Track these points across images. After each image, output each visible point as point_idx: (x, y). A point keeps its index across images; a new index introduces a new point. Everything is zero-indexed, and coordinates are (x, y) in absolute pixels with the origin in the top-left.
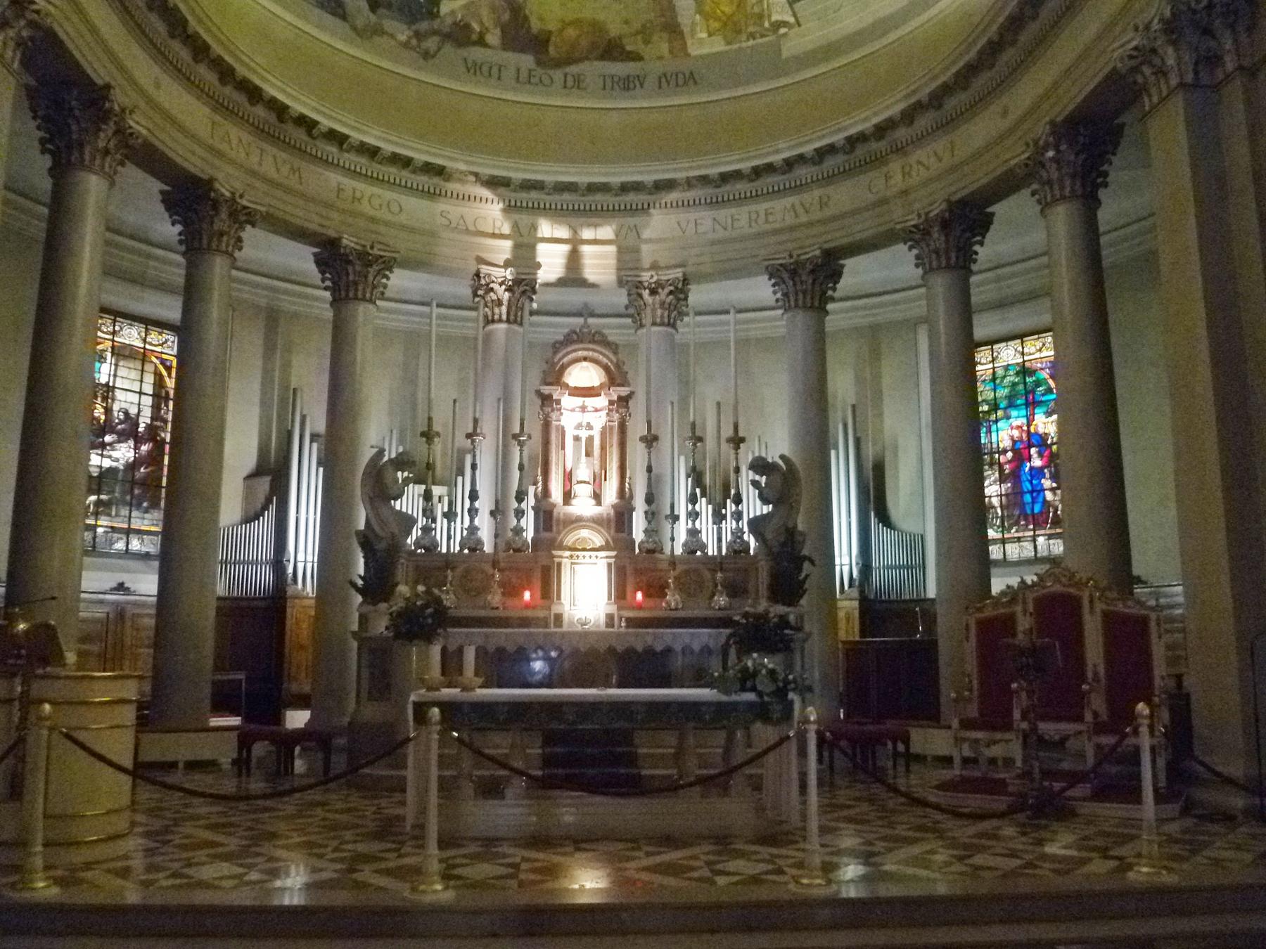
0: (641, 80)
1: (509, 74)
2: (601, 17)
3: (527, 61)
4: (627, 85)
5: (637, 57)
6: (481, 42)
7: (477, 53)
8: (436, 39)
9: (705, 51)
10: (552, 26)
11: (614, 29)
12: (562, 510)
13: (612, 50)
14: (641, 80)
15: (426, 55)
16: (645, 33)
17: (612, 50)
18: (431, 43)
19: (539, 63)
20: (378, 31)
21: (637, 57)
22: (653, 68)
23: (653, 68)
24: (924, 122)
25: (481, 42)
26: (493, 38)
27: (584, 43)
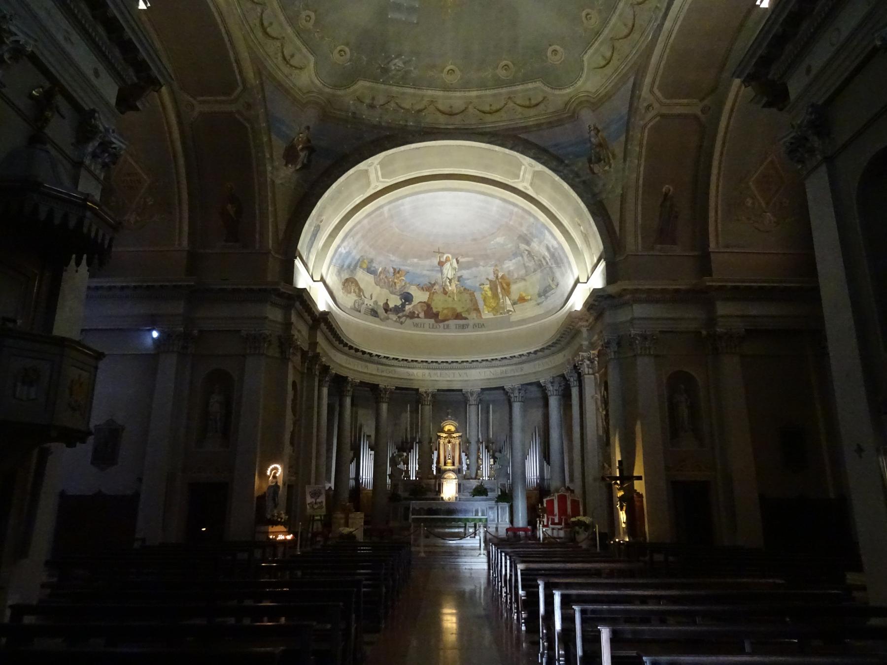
0: (468, 325)
1: (427, 326)
2: (455, 306)
3: (432, 321)
4: (463, 327)
5: (466, 319)
6: (418, 317)
7: (416, 320)
10: (440, 310)
11: (459, 310)
12: (444, 467)
13: (458, 316)
14: (468, 325)
15: (402, 323)
17: (458, 316)
18: (403, 319)
19: (436, 322)
20: (388, 318)
21: (466, 319)
22: (471, 322)
24: (547, 352)
26: (422, 315)
27: (450, 314)
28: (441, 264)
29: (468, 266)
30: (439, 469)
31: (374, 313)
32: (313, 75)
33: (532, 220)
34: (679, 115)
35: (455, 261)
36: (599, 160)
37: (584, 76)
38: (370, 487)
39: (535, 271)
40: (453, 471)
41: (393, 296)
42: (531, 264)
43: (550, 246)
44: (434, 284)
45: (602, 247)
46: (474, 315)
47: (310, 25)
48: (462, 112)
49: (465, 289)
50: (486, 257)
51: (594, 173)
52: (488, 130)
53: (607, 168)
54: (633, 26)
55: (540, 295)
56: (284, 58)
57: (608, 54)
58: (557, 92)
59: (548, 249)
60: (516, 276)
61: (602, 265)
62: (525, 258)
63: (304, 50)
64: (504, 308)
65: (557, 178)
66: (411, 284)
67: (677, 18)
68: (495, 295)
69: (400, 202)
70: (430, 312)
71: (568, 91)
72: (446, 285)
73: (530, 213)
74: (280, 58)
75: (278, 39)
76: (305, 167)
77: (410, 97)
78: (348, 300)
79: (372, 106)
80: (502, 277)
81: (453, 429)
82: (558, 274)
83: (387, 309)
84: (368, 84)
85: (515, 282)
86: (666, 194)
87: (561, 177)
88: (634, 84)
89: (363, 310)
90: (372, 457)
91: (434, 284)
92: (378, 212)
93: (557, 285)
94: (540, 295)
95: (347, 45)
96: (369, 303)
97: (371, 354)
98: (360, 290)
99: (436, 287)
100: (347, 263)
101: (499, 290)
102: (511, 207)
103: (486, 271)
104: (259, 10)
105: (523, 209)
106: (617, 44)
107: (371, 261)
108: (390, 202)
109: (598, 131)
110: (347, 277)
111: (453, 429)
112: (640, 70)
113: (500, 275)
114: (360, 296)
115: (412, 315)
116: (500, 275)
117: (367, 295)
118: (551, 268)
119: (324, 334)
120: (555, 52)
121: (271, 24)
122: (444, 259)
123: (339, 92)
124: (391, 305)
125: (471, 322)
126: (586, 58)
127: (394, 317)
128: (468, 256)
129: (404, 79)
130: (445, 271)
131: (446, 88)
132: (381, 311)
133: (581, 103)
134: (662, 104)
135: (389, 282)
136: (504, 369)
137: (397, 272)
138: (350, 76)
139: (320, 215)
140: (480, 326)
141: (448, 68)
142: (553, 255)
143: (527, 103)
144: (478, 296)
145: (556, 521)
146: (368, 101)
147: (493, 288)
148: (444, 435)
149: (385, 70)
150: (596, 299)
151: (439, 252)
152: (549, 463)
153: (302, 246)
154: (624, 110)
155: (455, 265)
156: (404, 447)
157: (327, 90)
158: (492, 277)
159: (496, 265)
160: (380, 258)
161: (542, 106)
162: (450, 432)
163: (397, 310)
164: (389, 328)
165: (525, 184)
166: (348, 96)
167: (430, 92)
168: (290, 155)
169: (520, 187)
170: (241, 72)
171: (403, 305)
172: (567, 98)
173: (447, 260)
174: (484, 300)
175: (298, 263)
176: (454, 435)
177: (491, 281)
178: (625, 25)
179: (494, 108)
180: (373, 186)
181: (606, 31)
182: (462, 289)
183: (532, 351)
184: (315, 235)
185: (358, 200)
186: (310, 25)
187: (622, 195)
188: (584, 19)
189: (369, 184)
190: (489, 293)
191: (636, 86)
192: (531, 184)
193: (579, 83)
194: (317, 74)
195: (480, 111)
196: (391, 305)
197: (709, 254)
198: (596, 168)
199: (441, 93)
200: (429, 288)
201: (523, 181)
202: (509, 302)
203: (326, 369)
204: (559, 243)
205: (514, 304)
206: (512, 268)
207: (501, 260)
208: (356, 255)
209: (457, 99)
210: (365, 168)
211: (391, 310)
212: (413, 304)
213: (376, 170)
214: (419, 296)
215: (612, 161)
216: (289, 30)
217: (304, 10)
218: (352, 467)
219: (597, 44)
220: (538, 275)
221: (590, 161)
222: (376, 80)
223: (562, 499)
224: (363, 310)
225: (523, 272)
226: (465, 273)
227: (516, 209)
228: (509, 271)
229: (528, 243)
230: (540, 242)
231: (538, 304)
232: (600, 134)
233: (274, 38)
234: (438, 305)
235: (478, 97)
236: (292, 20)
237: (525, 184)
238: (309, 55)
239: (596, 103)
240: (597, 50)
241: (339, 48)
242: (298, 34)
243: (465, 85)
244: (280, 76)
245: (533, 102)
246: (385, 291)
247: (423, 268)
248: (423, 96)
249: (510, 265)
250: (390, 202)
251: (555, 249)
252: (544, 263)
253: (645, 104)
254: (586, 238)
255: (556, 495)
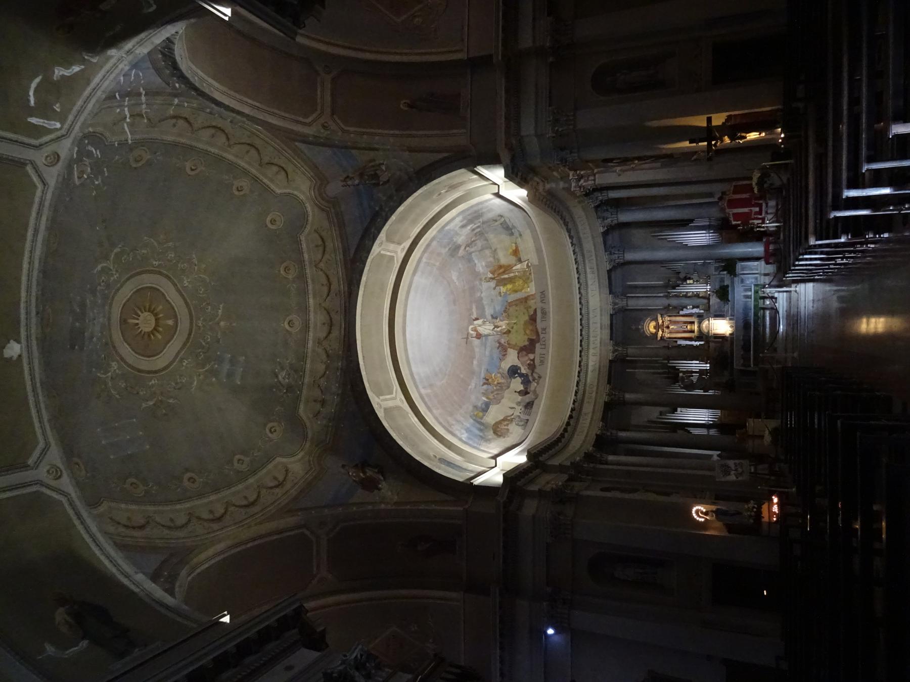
1: (544, 352)
2: (522, 322)
3: (538, 345)
4: (544, 313)
5: (535, 310)
6: (533, 360)
7: (537, 362)
8: (535, 375)
9: (534, 289)
10: (526, 337)
11: (527, 318)
12: (696, 333)
13: (533, 319)
15: (540, 377)
16: (527, 308)
17: (533, 319)
18: (535, 375)
20: (535, 391)
21: (535, 310)
22: (540, 305)
23: (539, 305)
24: (570, 226)
25: (533, 360)
26: (531, 356)
27: (531, 328)
28: (479, 336)
29: (481, 308)
30: (698, 338)
31: (529, 406)
32: (292, 459)
33: (434, 243)
34: (332, 95)
35: (476, 322)
36: (375, 176)
37: (295, 193)
38: (718, 412)
39: (486, 240)
40: (700, 323)
41: (512, 385)
42: (480, 244)
43: (461, 224)
44: (500, 343)
45: (463, 170)
46: (531, 303)
47: (247, 460)
48: (328, 313)
49: (505, 311)
50: (473, 289)
51: (388, 181)
52: (346, 289)
53: (384, 168)
54: (249, 144)
55: (512, 234)
56: (277, 487)
57: (275, 169)
58: (310, 218)
59: (463, 226)
60: (491, 259)
61: (482, 170)
62: (472, 250)
63: (270, 466)
64: (525, 272)
65: (393, 217)
66: (500, 367)
67: (241, 101)
68: (511, 280)
69: (416, 377)
70: (528, 348)
71: (309, 209)
72: (500, 331)
73: (428, 245)
74: (277, 490)
75: (259, 492)
76: (381, 472)
77: (315, 366)
78: (516, 432)
79: (323, 403)
80: (493, 273)
81: (653, 324)
82: (490, 215)
83: (525, 393)
84: (302, 407)
85: (498, 260)
86: (411, 106)
87: (391, 215)
88: (304, 142)
89: (527, 417)
90: (684, 410)
91: (500, 343)
92: (427, 400)
93: (501, 216)
94: (512, 234)
95: (265, 425)
96: (518, 410)
97: (573, 410)
98: (503, 420)
99: (503, 341)
100: (477, 432)
101: (506, 276)
102: (422, 265)
103: (486, 289)
104: (232, 509)
105: (424, 251)
106: (266, 159)
107: (475, 407)
108: (417, 387)
109: (348, 177)
110: (492, 432)
111: (653, 324)
112: (289, 138)
113: (490, 275)
114: (511, 420)
115: (532, 366)
116: (490, 275)
117: (510, 412)
118: (483, 223)
119: (553, 456)
120: (273, 222)
121: (245, 498)
122: (474, 333)
123: (310, 435)
124: (521, 388)
125: (540, 305)
126: (278, 191)
127: (534, 384)
128: (471, 309)
129: (297, 370)
130: (486, 332)
131: (306, 327)
132: (527, 398)
133: (320, 194)
134: (322, 112)
135: (497, 390)
136: (588, 270)
137: (487, 382)
138: (294, 423)
139: (428, 458)
140: (543, 295)
141: (287, 326)
142: (470, 221)
143: (321, 249)
144: (512, 297)
145: (757, 209)
146: (318, 406)
147: (502, 282)
148: (660, 332)
149: (290, 388)
150: (515, 175)
151: (467, 338)
152: (692, 221)
153: (460, 477)
154: (328, 152)
155: (480, 322)
156: (674, 376)
157: (308, 445)
158: (492, 284)
159: (481, 280)
160: (473, 397)
161: (324, 234)
162: (657, 327)
163: (526, 381)
164: (544, 391)
165: (399, 251)
166: (314, 427)
167: (310, 344)
168: (370, 485)
169: (401, 255)
170: (291, 529)
171: (521, 375)
172: (316, 210)
173: (475, 330)
174: (516, 291)
175: (478, 481)
176: (660, 322)
177: (497, 285)
178: (248, 152)
179: (325, 281)
180: (400, 404)
181: (254, 171)
182: (504, 315)
183: (569, 241)
184: (449, 464)
185: (415, 420)
186: (247, 460)
187: (410, 151)
188: (242, 193)
189: (398, 408)
190: (509, 286)
191: (305, 140)
192: (399, 244)
193: (302, 197)
194: (292, 455)
195: (328, 295)
196: (521, 388)
197: (469, 59)
198: (384, 178)
199: (311, 334)
200: (503, 349)
201: (396, 252)
202: (519, 266)
203: (588, 456)
204: (458, 215)
205: (520, 261)
206: (484, 264)
207: (475, 274)
208: (469, 423)
209: (316, 318)
210: (382, 410)
211: (526, 388)
212: (520, 365)
213: (383, 400)
214: (512, 359)
215: (377, 162)
216: (251, 481)
217: (233, 465)
218: (696, 431)
219: (265, 181)
220: (491, 236)
221: (378, 184)
222: (298, 398)
223: (733, 204)
224: (527, 417)
225: (487, 252)
226: (489, 311)
227: (424, 260)
228: (487, 266)
229: (458, 247)
230: (457, 234)
231: (521, 235)
232: (351, 175)
233: (258, 496)
234: (521, 339)
235: (314, 297)
236: (242, 477)
237: (399, 251)
238: (274, 463)
239: (321, 180)
240: (272, 180)
241: (267, 431)
242: (254, 472)
243: (304, 309)
244: (293, 492)
245: (320, 242)
246: (507, 394)
247: (483, 353)
248: (313, 351)
249: (480, 266)
250: (417, 387)
251: (464, 218)
252: (478, 230)
253: (322, 131)
254: (453, 187)
255: (727, 210)
